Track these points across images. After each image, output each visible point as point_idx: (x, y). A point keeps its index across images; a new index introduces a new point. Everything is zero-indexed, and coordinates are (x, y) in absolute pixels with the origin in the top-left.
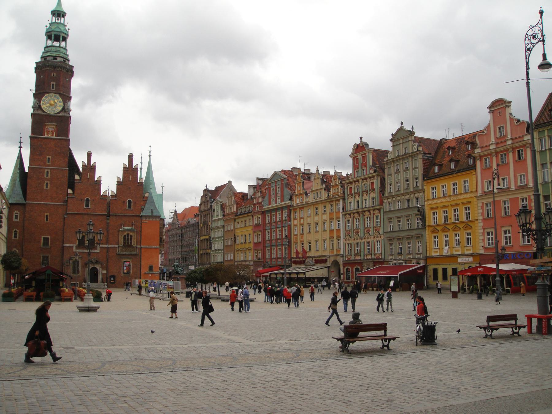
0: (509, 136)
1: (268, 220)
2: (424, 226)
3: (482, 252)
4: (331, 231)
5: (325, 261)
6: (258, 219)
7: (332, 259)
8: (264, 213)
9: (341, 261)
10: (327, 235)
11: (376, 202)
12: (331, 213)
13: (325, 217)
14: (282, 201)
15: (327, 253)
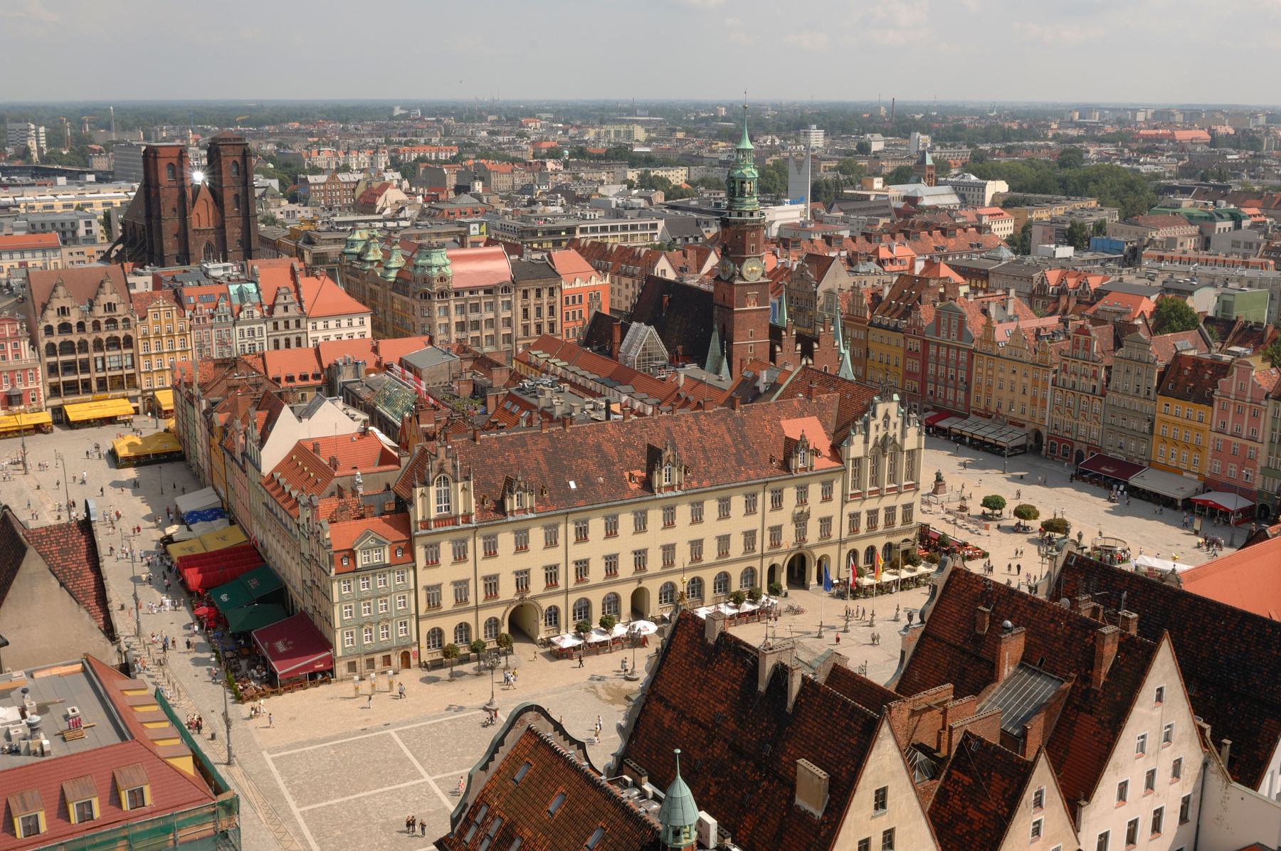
0: (1249, 394)
1: (933, 350)
2: (1152, 433)
3: (1208, 475)
4: (1034, 398)
5: (1023, 426)
6: (915, 344)
7: (1033, 426)
8: (926, 344)
9: (1044, 432)
10: (1027, 399)
11: (1098, 391)
12: (1035, 380)
13: (1025, 380)
14: (960, 338)
15: (1026, 417)
